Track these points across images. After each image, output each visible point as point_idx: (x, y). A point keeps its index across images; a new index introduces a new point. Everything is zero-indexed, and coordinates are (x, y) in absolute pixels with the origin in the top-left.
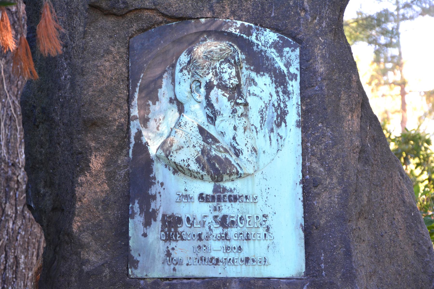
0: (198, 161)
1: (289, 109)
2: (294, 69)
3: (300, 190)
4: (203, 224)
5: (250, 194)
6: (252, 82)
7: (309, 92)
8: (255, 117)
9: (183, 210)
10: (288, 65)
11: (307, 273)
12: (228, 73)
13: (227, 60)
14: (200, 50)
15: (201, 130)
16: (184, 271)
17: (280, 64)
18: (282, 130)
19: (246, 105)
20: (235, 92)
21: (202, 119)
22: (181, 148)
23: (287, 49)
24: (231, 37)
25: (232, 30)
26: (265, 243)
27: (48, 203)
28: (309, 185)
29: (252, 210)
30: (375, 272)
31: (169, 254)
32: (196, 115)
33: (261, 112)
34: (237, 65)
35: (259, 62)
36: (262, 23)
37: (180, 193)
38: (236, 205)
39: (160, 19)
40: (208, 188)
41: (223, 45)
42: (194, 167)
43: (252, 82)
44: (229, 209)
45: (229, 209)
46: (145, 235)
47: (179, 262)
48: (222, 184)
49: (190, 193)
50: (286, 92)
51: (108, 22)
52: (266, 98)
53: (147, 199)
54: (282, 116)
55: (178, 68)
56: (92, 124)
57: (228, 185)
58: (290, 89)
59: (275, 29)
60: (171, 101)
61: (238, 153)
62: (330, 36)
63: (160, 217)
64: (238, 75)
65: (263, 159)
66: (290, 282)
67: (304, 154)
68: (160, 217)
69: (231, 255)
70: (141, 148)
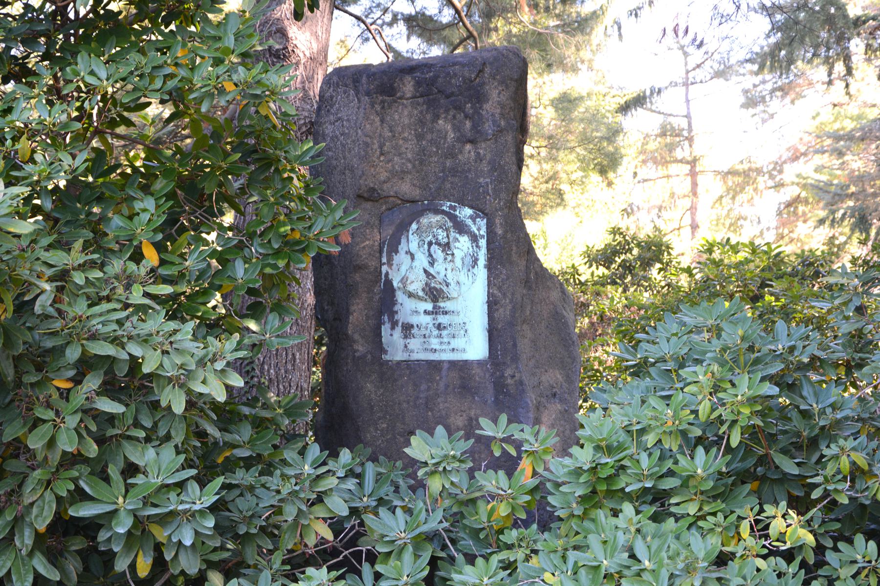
0: (423, 290)
1: (479, 257)
2: (483, 232)
3: (486, 307)
4: (427, 328)
5: (455, 310)
6: (457, 240)
7: (492, 246)
8: (458, 262)
9: (414, 320)
10: (479, 229)
11: (490, 357)
12: (442, 235)
13: (441, 227)
14: (424, 221)
15: (425, 271)
16: (415, 356)
17: (474, 229)
18: (475, 270)
19: (453, 254)
20: (446, 247)
22: (412, 282)
23: (478, 220)
24: (443, 212)
25: (444, 208)
26: (464, 340)
27: (330, 315)
28: (492, 304)
29: (456, 320)
30: (533, 356)
31: (406, 346)
32: (422, 260)
33: (462, 259)
34: (447, 230)
35: (461, 228)
36: (463, 203)
37: (412, 309)
38: (447, 317)
39: (400, 202)
40: (429, 306)
41: (439, 217)
42: (421, 294)
43: (457, 240)
44: (442, 319)
46: (391, 335)
47: (412, 351)
48: (438, 304)
49: (419, 310)
50: (478, 246)
51: (368, 205)
52: (466, 250)
53: (392, 314)
54: (475, 261)
56: (359, 268)
57: (442, 304)
58: (480, 244)
59: (471, 207)
60: (407, 253)
62: (506, 211)
63: (400, 324)
64: (448, 236)
65: (464, 288)
66: (479, 363)
67: (489, 285)
68: (400, 324)
69: (444, 347)
70: (389, 283)
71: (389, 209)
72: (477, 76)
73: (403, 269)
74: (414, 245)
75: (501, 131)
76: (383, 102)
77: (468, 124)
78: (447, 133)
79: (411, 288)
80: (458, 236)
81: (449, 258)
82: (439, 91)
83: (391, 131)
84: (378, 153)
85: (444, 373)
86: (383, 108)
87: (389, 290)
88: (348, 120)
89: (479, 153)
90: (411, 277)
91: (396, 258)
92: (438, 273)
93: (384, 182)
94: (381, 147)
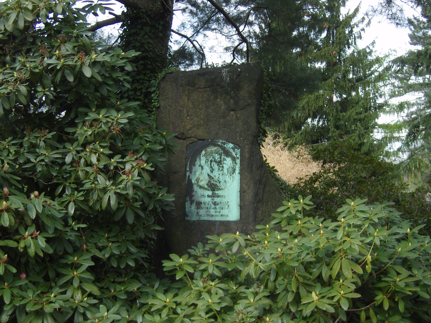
0: (207, 185)
1: (236, 168)
2: (238, 156)
3: (239, 194)
4: (208, 204)
8: (225, 171)
9: (202, 200)
10: (236, 154)
12: (217, 157)
13: (217, 153)
14: (209, 150)
15: (209, 175)
16: (203, 218)
17: (234, 154)
18: (234, 175)
19: (223, 167)
21: (209, 172)
22: (202, 181)
23: (236, 149)
24: (218, 146)
25: (219, 143)
26: (227, 210)
29: (224, 200)
31: (198, 213)
32: (207, 169)
33: (228, 169)
35: (227, 154)
38: (219, 199)
39: (196, 140)
41: (216, 148)
42: (206, 186)
44: (217, 200)
45: (217, 200)
46: (191, 207)
47: (201, 216)
49: (204, 194)
50: (236, 163)
52: (229, 165)
53: (191, 196)
54: (234, 170)
55: (202, 155)
57: (217, 192)
58: (237, 162)
61: (220, 182)
63: (195, 202)
64: (220, 158)
65: (228, 184)
66: (235, 222)
68: (195, 202)
69: (217, 214)
70: (190, 181)
71: (191, 143)
72: (237, 77)
73: (198, 174)
74: (203, 162)
75: (248, 105)
76: (189, 89)
77: (232, 101)
78: (221, 106)
79: (201, 184)
80: (225, 157)
81: (221, 169)
82: (217, 85)
83: (193, 104)
84: (186, 115)
85: (217, 227)
86: (189, 93)
87: (190, 185)
88: (172, 99)
89: (237, 116)
90: (201, 178)
91: (194, 169)
92: (215, 176)
93: (189, 130)
94: (187, 112)
